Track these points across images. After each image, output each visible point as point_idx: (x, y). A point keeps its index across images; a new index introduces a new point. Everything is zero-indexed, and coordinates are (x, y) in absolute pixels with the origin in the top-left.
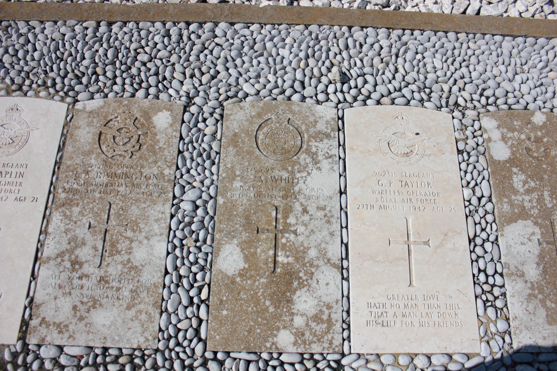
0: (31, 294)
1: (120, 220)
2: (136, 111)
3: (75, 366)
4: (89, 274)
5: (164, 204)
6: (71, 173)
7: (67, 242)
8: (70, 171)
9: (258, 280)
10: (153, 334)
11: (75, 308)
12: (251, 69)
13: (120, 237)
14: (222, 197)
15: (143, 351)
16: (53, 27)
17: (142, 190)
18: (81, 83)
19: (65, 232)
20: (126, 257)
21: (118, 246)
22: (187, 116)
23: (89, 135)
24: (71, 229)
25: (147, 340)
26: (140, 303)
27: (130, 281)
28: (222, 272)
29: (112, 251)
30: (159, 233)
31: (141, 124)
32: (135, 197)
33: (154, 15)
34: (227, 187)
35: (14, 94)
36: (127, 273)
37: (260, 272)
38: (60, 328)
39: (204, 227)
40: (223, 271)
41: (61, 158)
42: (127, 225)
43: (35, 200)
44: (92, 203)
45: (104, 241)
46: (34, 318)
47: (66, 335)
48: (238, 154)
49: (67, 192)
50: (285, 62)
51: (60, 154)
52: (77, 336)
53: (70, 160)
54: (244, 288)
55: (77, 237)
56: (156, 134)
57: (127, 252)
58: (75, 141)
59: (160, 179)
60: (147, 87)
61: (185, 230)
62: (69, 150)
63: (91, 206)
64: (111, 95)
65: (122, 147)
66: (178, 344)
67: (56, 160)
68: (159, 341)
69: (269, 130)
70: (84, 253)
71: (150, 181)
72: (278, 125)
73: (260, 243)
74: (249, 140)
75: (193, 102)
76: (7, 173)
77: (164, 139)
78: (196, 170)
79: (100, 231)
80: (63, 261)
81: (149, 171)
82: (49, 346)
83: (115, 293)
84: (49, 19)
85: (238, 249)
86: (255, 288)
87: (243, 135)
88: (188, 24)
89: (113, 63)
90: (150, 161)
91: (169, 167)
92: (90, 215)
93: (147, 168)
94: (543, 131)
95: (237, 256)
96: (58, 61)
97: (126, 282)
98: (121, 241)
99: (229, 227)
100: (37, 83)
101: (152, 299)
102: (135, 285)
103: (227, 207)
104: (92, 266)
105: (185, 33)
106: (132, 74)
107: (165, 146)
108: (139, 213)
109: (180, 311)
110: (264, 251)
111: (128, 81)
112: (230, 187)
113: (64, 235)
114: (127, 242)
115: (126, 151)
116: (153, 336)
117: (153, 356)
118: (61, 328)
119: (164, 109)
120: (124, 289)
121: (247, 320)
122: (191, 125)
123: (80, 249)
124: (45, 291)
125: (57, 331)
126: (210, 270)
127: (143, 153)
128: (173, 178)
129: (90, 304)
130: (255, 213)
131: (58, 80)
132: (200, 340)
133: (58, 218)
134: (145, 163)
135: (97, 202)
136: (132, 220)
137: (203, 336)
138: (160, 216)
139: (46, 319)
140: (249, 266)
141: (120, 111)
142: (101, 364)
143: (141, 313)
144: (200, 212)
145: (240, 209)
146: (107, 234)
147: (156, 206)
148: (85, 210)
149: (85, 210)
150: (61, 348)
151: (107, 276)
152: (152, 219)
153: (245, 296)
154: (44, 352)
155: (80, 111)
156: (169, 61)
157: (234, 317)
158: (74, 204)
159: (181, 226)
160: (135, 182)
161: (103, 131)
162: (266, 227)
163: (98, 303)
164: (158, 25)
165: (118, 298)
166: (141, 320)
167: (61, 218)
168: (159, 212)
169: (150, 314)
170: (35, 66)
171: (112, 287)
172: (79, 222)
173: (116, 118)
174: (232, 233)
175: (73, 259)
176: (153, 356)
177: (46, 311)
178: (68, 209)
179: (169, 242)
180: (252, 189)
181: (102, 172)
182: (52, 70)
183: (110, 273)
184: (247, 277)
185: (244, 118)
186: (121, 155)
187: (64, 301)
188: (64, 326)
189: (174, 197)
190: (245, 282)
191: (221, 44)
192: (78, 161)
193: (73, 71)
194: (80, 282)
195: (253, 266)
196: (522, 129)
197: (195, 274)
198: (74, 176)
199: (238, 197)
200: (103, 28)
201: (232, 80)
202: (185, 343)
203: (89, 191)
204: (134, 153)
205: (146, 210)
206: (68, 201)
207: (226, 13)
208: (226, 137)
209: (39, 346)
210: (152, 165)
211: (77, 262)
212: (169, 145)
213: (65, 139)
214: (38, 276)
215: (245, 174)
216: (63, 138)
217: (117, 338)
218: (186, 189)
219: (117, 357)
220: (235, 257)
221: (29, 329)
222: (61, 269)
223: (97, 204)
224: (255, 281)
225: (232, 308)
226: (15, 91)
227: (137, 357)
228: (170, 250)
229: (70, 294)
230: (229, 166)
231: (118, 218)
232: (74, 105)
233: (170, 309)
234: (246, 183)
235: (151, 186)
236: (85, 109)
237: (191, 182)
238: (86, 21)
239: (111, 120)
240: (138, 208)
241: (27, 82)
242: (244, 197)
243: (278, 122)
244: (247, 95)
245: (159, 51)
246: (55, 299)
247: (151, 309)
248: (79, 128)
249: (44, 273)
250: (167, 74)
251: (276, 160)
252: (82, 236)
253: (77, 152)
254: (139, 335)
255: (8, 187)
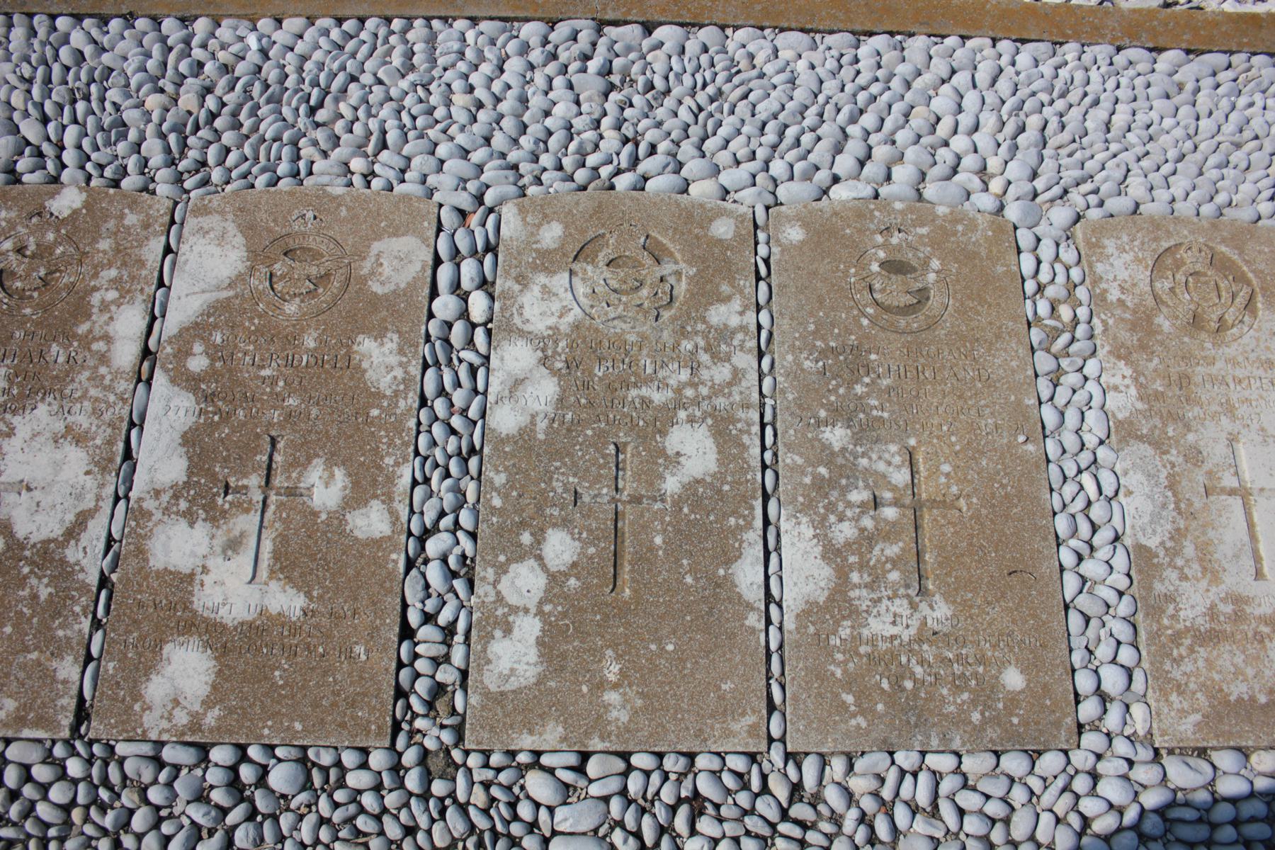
94: (63, 231)
196: (14, 228)
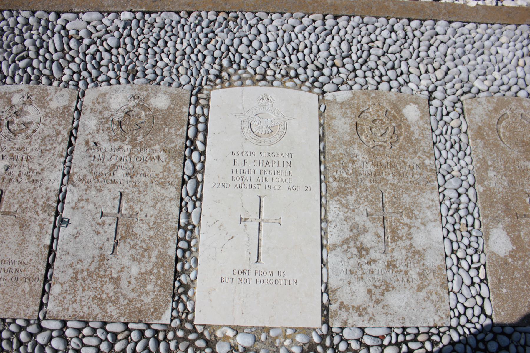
0: (325, 280)
1: (395, 208)
2: (385, 104)
3: (378, 345)
4: (377, 259)
5: (432, 193)
6: (338, 163)
7: (349, 230)
8: (337, 161)
9: (527, 260)
10: (446, 312)
11: (369, 291)
12: (478, 67)
13: (398, 224)
14: (482, 186)
15: (438, 329)
16: (281, 18)
17: (410, 179)
18: (322, 75)
19: (345, 220)
20: (408, 242)
21: (399, 232)
22: (432, 110)
23: (346, 125)
24: (350, 217)
25: (442, 318)
26: (429, 285)
27: (416, 265)
28: (495, 254)
29: (394, 237)
30: (433, 220)
31: (393, 116)
32: (404, 185)
33: (377, 10)
34: (483, 176)
35: (260, 84)
36: (411, 257)
37: (527, 254)
38: (359, 311)
39: (469, 213)
40: (495, 252)
41: (324, 147)
42: (402, 212)
43: (309, 189)
44: (365, 192)
45: (384, 228)
46: (332, 302)
47: (367, 317)
48: (485, 146)
49: (339, 181)
50: (506, 61)
51: (322, 144)
52: (377, 317)
53: (334, 150)
54: (516, 268)
55: (358, 225)
56: (409, 126)
57: (408, 238)
58: (334, 131)
59: (423, 169)
60: (388, 80)
61: (455, 216)
62: (330, 140)
63: (365, 194)
64: (355, 87)
65: (380, 138)
66: (468, 321)
67: (320, 150)
68: (451, 319)
69: (507, 124)
70: (368, 240)
71: (415, 171)
72: (514, 119)
73: (522, 227)
74: (492, 133)
75: (433, 96)
76: (274, 162)
77: (418, 132)
78: (452, 160)
79: (379, 219)
80: (349, 247)
81: (411, 161)
82: (352, 329)
83: (404, 276)
84: (275, 11)
85: (504, 233)
86: (526, 267)
87: (486, 129)
88: (410, 20)
89: (349, 56)
90: (410, 151)
91: (429, 157)
92: (366, 203)
93: (409, 158)
95: (505, 239)
96: (295, 52)
97: (412, 266)
98: (400, 228)
99: (493, 212)
100: (280, 73)
101: (438, 280)
102: (421, 268)
103: (487, 194)
104: (378, 252)
105: (408, 29)
106: (369, 67)
107: (420, 138)
108: (411, 201)
109: (465, 290)
110: (527, 234)
111: (369, 74)
112: (486, 176)
113: (345, 222)
114: (406, 229)
115: (385, 142)
116: (446, 315)
117: (448, 333)
118: (361, 311)
119: (411, 102)
120: (411, 272)
121: (524, 297)
122: (438, 118)
123: (363, 236)
124: (337, 277)
125: (357, 314)
126: (483, 252)
127: (401, 144)
128: (434, 168)
129: (383, 287)
130: (512, 200)
131: (300, 71)
132: (486, 316)
133: (336, 206)
134: (406, 154)
135: (370, 190)
136: (406, 208)
137: (488, 312)
138: (431, 203)
139: (345, 304)
140: (517, 248)
141: (371, 103)
142: (401, 342)
143: (431, 294)
144: (463, 198)
145: (499, 196)
146: (385, 221)
147: (425, 194)
148: (360, 199)
149: (360, 199)
150: (362, 329)
151: (394, 261)
152: (424, 206)
153: (519, 275)
154: (346, 334)
155: (332, 102)
156: (401, 57)
157: (513, 294)
158: (348, 192)
159: (451, 212)
160: (401, 172)
161: (358, 122)
162: (524, 213)
163: (391, 286)
164: (382, 20)
165: (408, 281)
166: (432, 300)
167: (338, 206)
168: (429, 199)
169: (440, 294)
170: (274, 56)
171: (401, 271)
172: (356, 210)
173: (367, 109)
174: (497, 219)
175: (359, 246)
176: (448, 333)
177: (343, 296)
178: (343, 198)
179: (443, 227)
180: (504, 178)
181: (367, 161)
182: (291, 61)
183: (396, 257)
184: (517, 258)
185: (484, 113)
186: (381, 146)
187: (358, 285)
188: (363, 309)
189: (439, 186)
190: (516, 263)
191: (445, 41)
192: (342, 151)
193: (312, 63)
194: (369, 267)
195: (520, 248)
197: (471, 256)
198: (341, 166)
199: (494, 185)
200: (330, 22)
201: (464, 76)
202: (475, 320)
203: (360, 181)
204: (393, 144)
205: (417, 198)
206: (342, 190)
207: (444, 11)
208: (472, 130)
209: (342, 329)
210: (412, 155)
211: (363, 248)
212: (424, 137)
213: (323, 129)
214: (327, 262)
215: (496, 164)
216: (321, 128)
217: (414, 318)
218: (447, 178)
219: (416, 335)
220: (504, 240)
221: (330, 313)
222: (349, 255)
223: (370, 192)
224: (524, 261)
225: (509, 286)
226: (260, 81)
227: (433, 334)
228: (445, 235)
229: (362, 278)
230: (481, 157)
231: (393, 206)
232: (323, 96)
233: (456, 289)
234: (499, 172)
235: (416, 176)
236: (335, 100)
237: (450, 171)
238: (312, 14)
239: (363, 111)
240: (409, 196)
241: (269, 72)
242: (500, 186)
243: (514, 117)
244: (479, 91)
245: (390, 46)
246: (349, 284)
247: (439, 290)
248: (335, 118)
249: (333, 259)
250: (404, 68)
251: (519, 152)
252: (363, 223)
253: (338, 142)
254: (434, 314)
255: (279, 177)
